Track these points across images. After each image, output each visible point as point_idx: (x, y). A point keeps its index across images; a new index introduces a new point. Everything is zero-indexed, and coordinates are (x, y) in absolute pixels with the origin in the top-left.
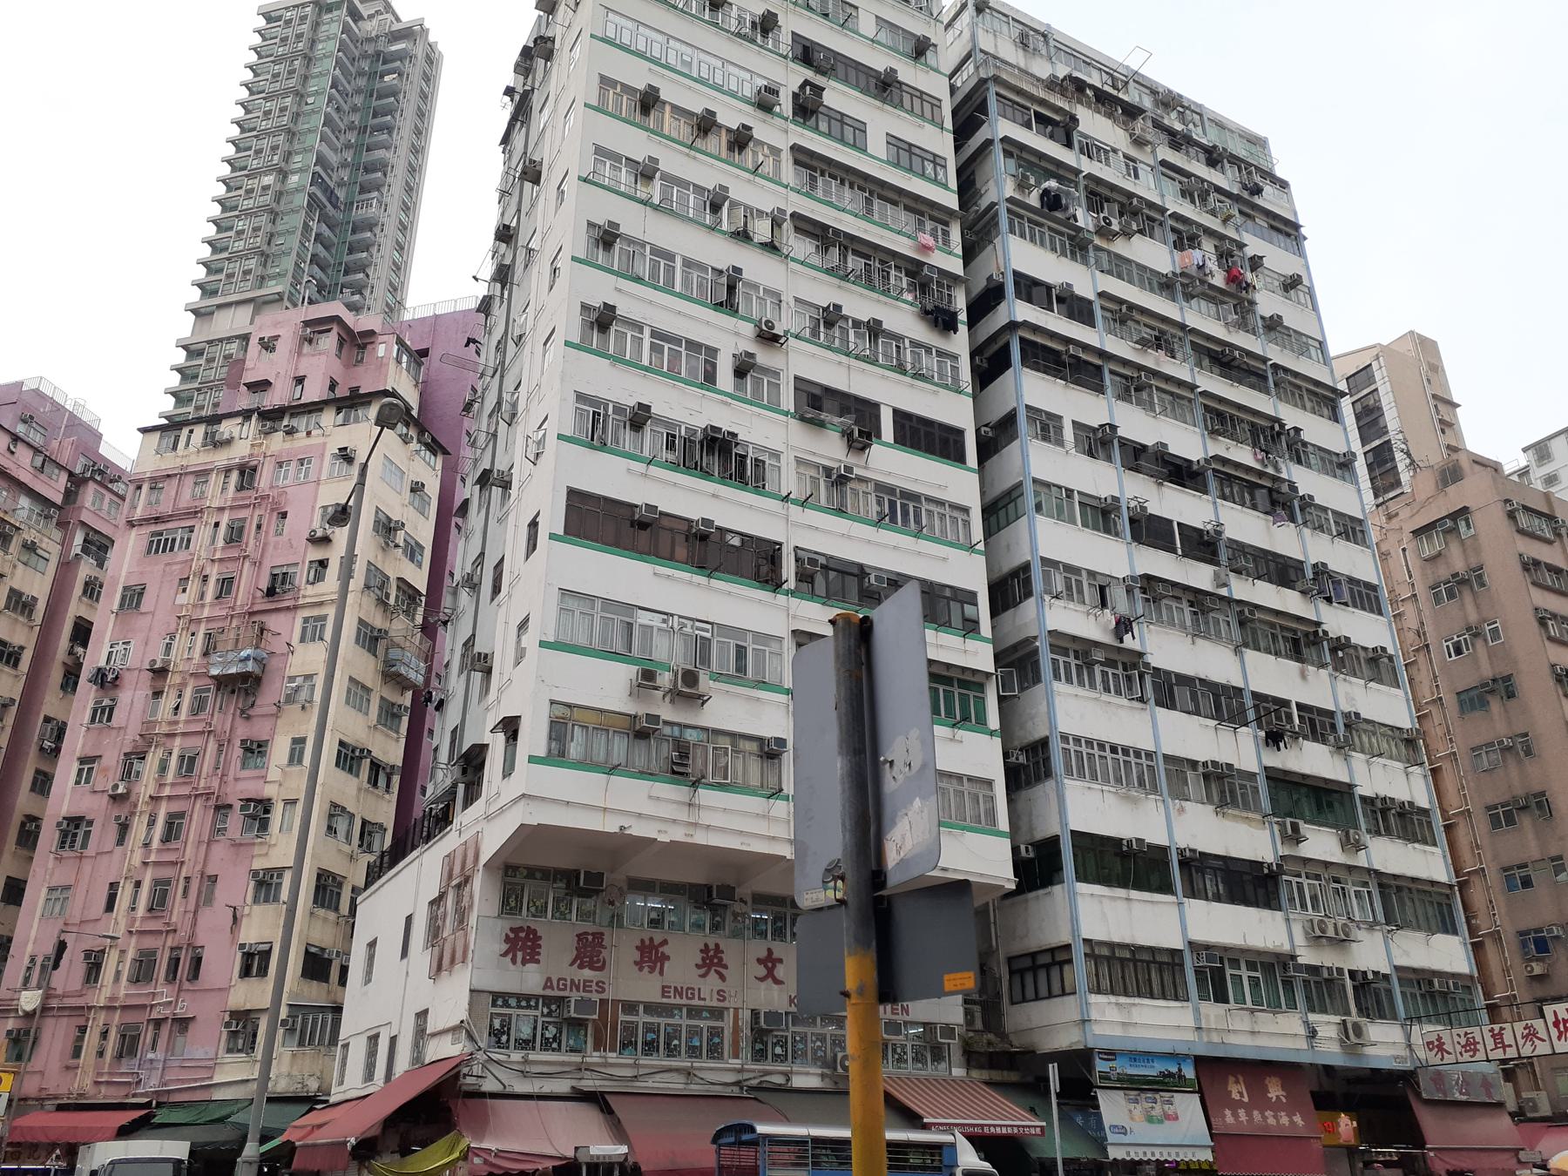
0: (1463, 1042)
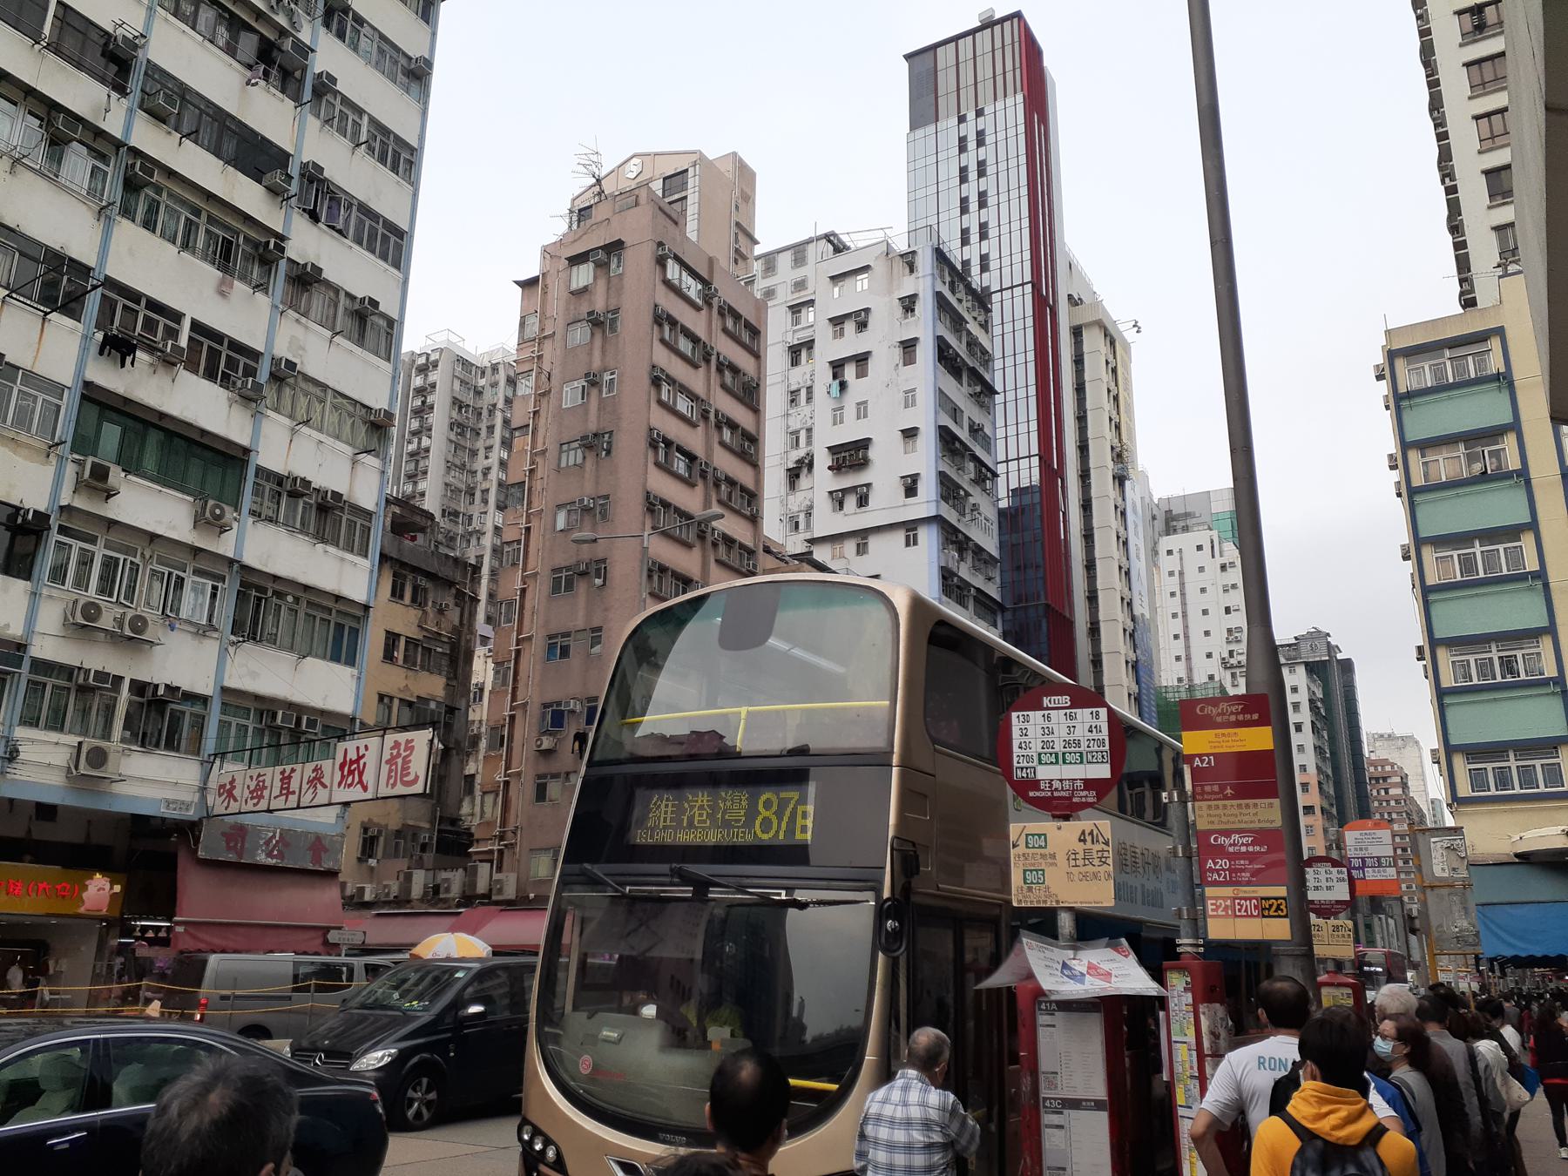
0: (253, 785)
